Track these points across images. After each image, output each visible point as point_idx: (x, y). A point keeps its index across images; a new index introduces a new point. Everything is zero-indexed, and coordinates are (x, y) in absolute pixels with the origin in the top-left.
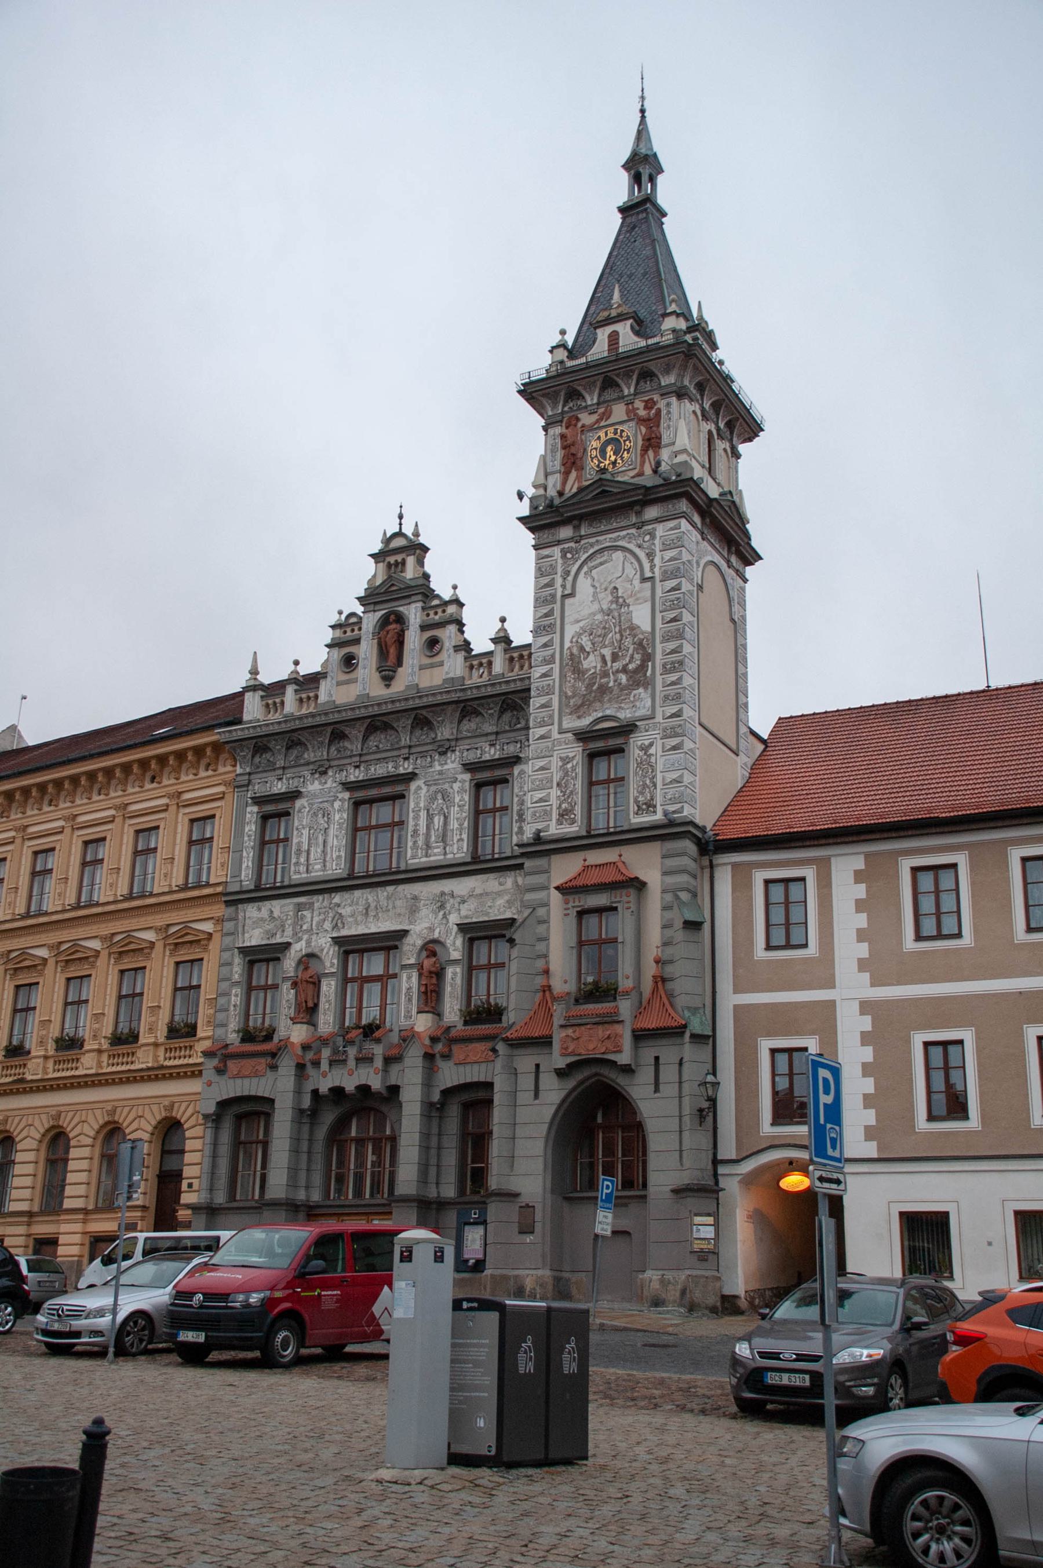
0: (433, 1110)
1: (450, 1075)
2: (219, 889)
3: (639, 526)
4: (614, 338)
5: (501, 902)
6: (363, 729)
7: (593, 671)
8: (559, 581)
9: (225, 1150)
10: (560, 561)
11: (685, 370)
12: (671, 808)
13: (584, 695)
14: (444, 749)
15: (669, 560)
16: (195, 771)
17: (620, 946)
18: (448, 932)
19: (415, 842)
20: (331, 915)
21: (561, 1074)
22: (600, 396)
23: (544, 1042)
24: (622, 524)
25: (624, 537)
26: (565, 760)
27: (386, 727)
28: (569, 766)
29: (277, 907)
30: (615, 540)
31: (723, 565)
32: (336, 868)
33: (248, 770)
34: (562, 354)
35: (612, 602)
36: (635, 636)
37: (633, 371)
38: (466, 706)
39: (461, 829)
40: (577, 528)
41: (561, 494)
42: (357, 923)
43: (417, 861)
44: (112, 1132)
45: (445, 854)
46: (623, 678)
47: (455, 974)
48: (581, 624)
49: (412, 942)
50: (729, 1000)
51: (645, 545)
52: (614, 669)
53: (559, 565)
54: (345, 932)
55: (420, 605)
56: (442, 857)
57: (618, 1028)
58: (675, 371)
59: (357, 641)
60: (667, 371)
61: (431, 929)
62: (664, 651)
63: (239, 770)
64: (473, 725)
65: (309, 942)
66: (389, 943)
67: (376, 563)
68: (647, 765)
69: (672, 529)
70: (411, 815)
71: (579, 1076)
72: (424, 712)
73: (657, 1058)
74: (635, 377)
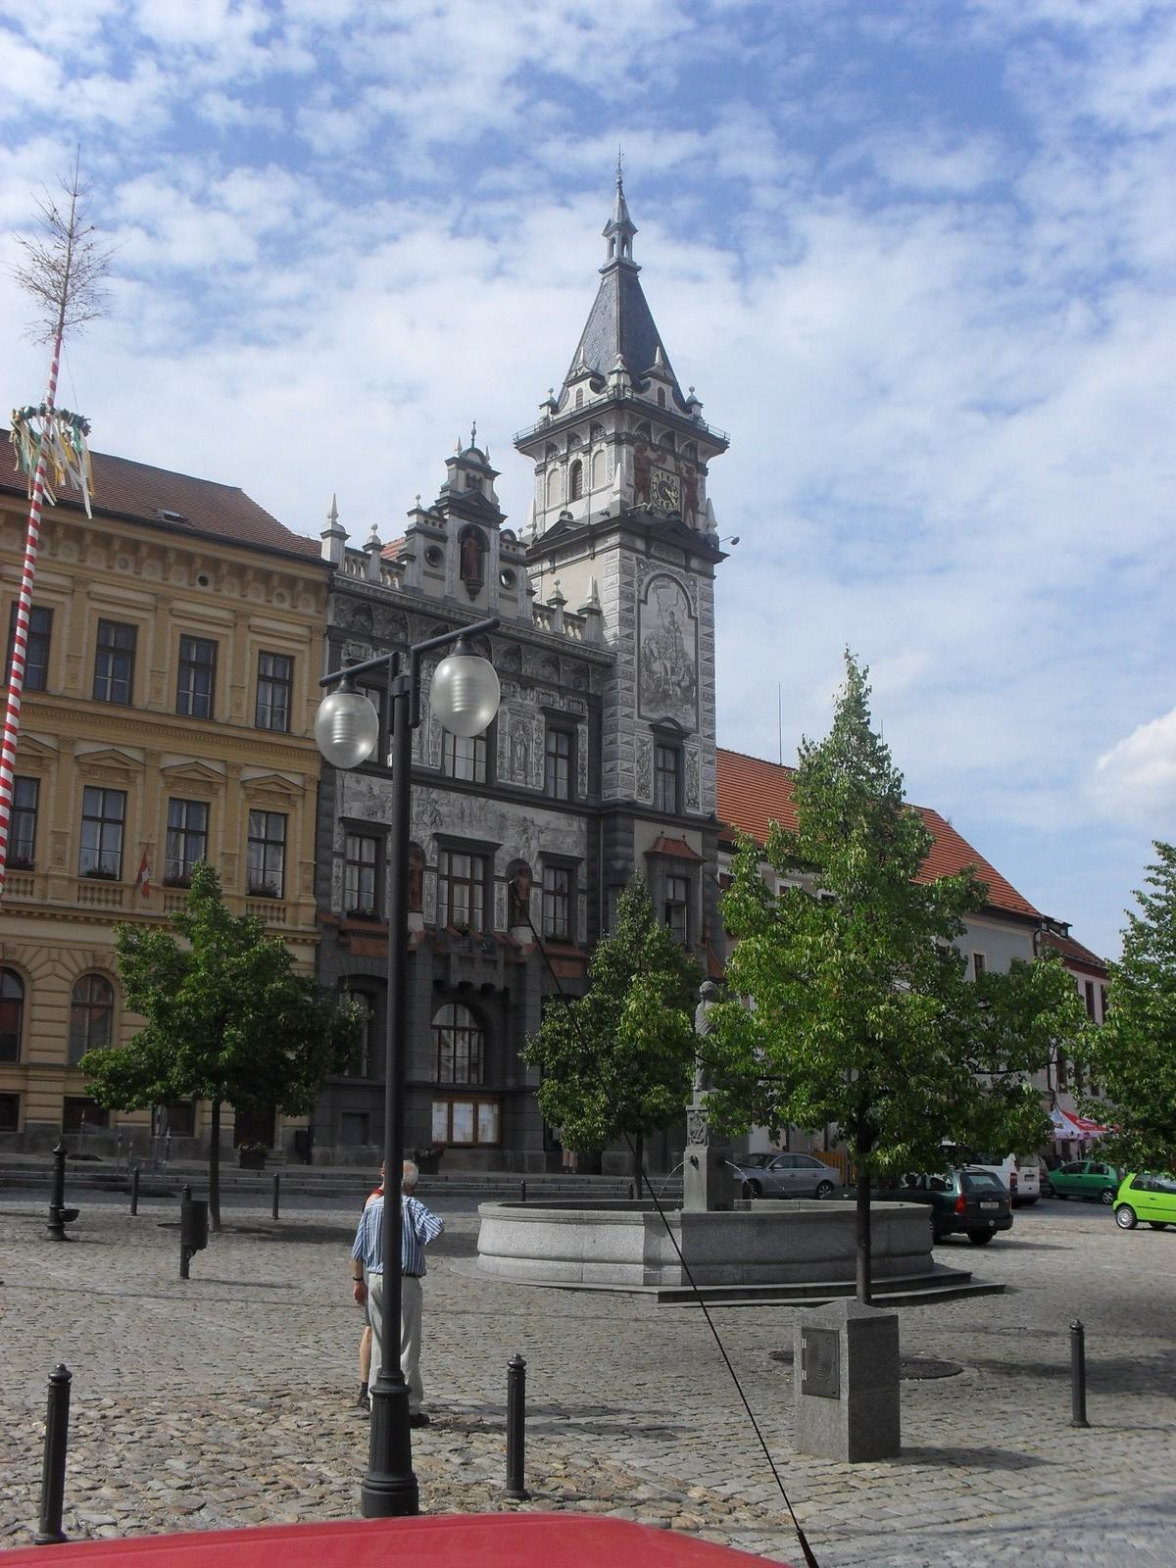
3: (687, 569)
8: (636, 585)
25: (677, 573)
26: (643, 743)
39: (538, 764)
40: (648, 546)
47: (536, 894)
54: (442, 830)
61: (517, 849)
63: (330, 622)
66: (483, 852)
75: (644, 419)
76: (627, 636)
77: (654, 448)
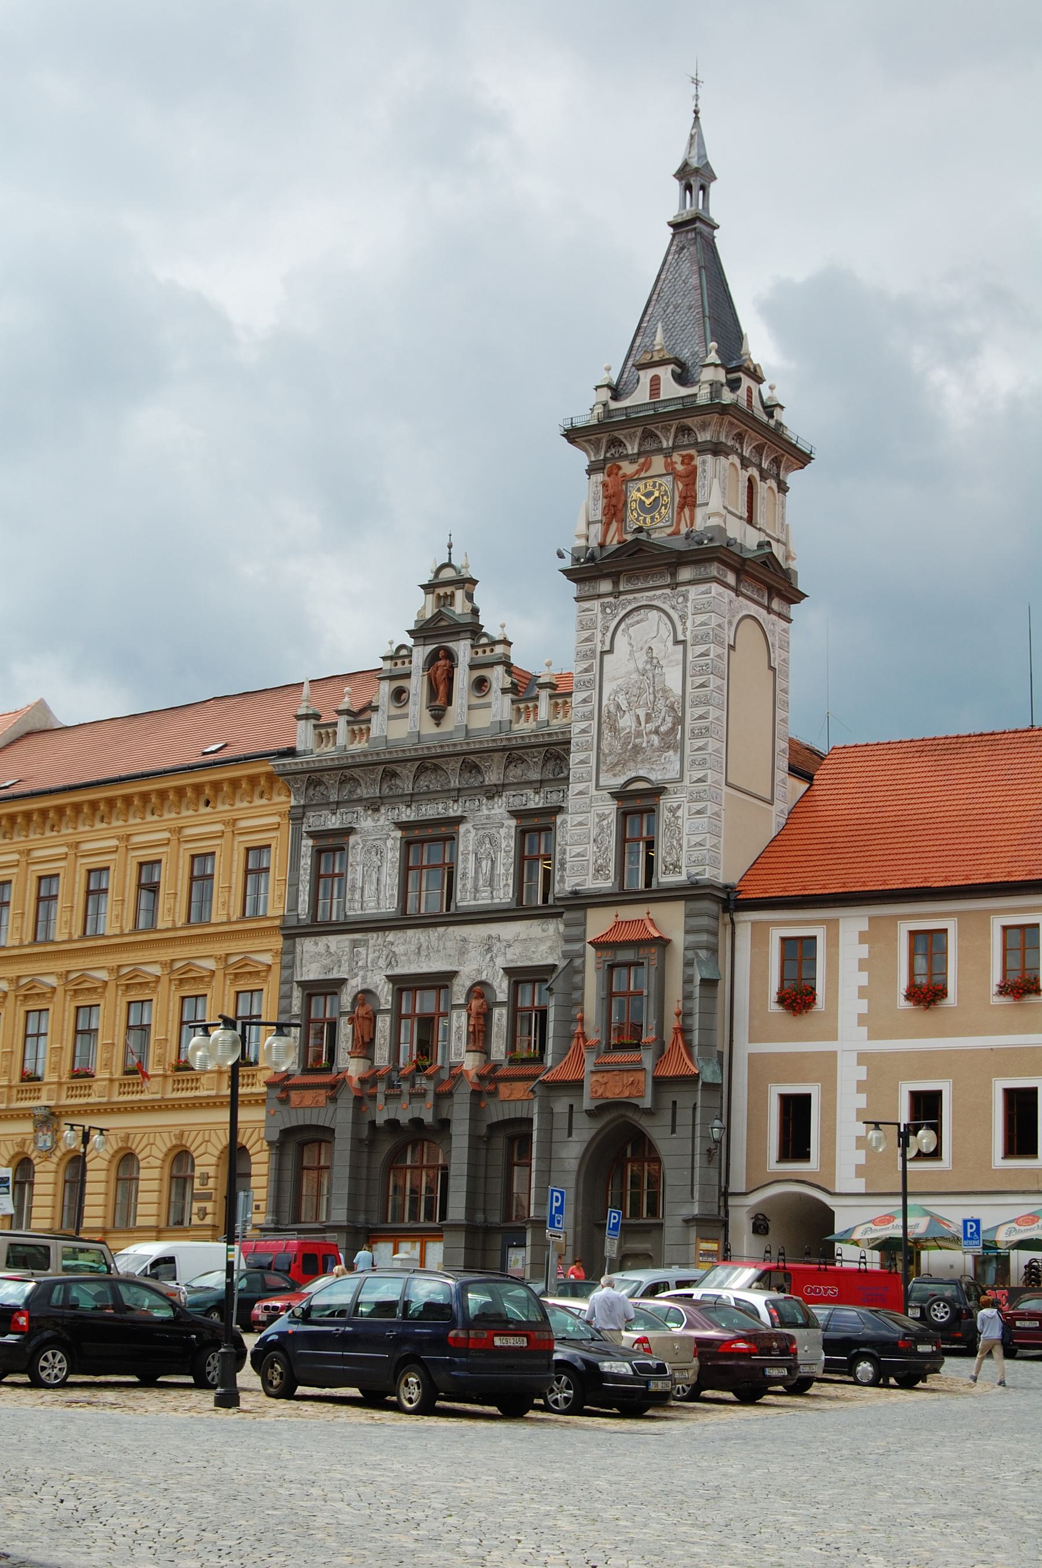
0: (478, 1142)
1: (497, 1112)
2: (277, 923)
3: (674, 586)
4: (655, 381)
6: (414, 769)
7: (628, 730)
8: (599, 636)
9: (289, 1175)
10: (600, 616)
11: (721, 426)
12: (694, 870)
13: (621, 754)
14: (493, 792)
15: (700, 625)
16: (249, 799)
17: (645, 999)
19: (464, 885)
21: (590, 1113)
22: (640, 445)
23: (577, 1085)
24: (658, 583)
26: (602, 817)
27: (436, 768)
28: (605, 822)
29: (334, 942)
30: (651, 599)
31: (761, 613)
32: (389, 906)
33: (302, 802)
34: (605, 394)
35: (647, 662)
36: (667, 699)
37: (671, 426)
38: (513, 753)
40: (616, 584)
41: (602, 546)
42: (409, 962)
43: (466, 903)
44: (181, 1157)
45: (492, 898)
46: (655, 739)
47: (501, 1015)
48: (619, 682)
49: (461, 983)
50: (744, 1048)
51: (679, 607)
52: (648, 730)
53: (599, 620)
54: (398, 971)
55: (469, 642)
56: (489, 901)
57: (640, 1076)
58: (712, 428)
59: (408, 676)
60: (704, 427)
61: (479, 971)
62: (692, 716)
63: (293, 803)
64: (519, 772)
65: (364, 978)
67: (426, 593)
68: (675, 828)
69: (703, 593)
70: (460, 857)
71: (606, 1118)
72: (471, 757)
73: (674, 1103)
74: (673, 430)
75: (605, 438)
77: (633, 459)
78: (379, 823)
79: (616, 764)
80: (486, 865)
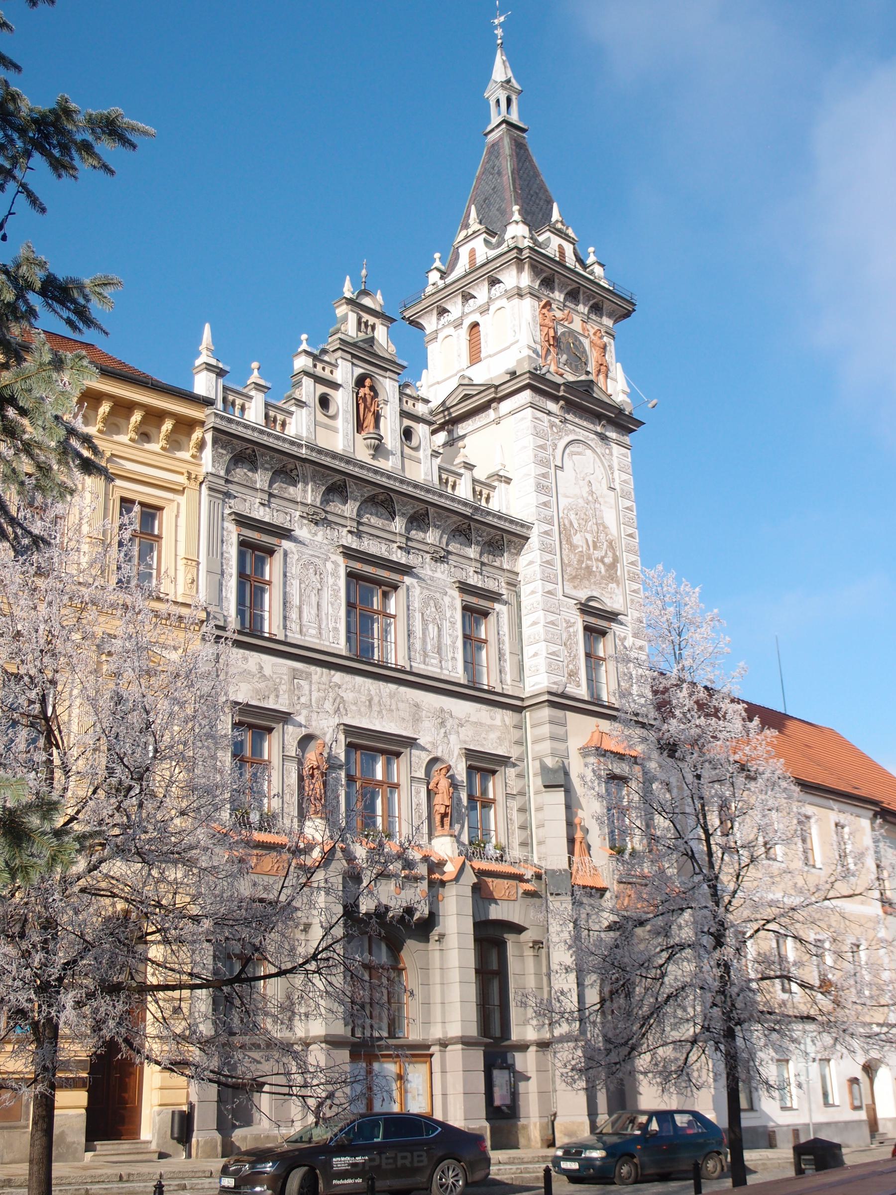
5: (493, 736)
7: (580, 549)
18: (450, 753)
20: (331, 694)
26: (570, 625)
28: (571, 630)
37: (594, 298)
45: (441, 668)
48: (570, 500)
65: (308, 718)
74: (591, 303)
76: (545, 504)
78: (315, 538)
79: (575, 577)
80: (432, 630)
